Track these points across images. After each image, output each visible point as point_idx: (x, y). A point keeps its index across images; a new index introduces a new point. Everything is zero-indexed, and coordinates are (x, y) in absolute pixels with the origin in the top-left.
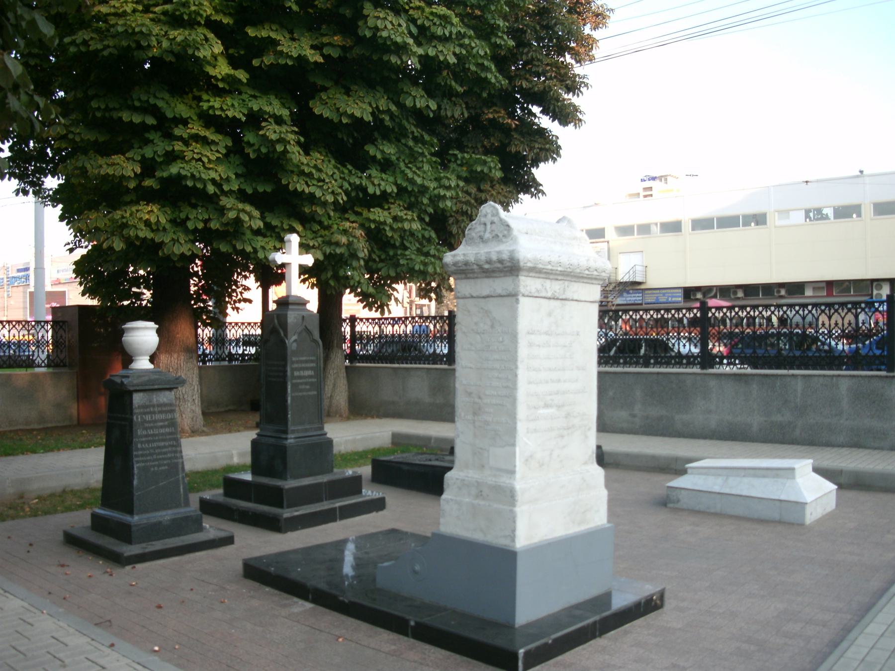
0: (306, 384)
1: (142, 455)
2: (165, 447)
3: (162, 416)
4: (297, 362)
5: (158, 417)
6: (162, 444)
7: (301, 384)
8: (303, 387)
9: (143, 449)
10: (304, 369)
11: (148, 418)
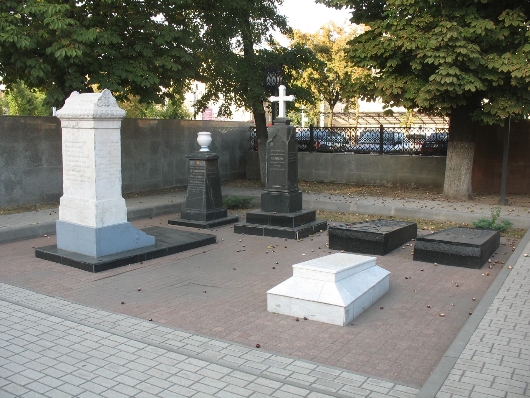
0: (278, 164)
1: (191, 186)
2: (199, 184)
3: (200, 171)
4: (273, 152)
5: (198, 171)
6: (198, 182)
7: (275, 164)
8: (277, 165)
9: (191, 183)
10: (277, 156)
11: (194, 171)
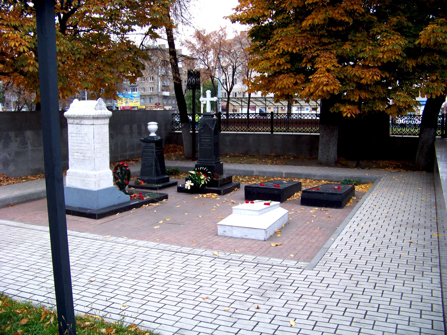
0: (207, 144)
3: (150, 150)
10: (206, 139)
11: (146, 150)
